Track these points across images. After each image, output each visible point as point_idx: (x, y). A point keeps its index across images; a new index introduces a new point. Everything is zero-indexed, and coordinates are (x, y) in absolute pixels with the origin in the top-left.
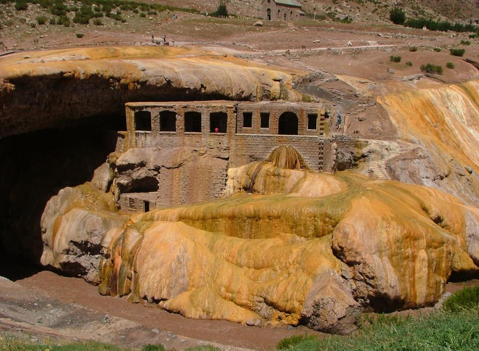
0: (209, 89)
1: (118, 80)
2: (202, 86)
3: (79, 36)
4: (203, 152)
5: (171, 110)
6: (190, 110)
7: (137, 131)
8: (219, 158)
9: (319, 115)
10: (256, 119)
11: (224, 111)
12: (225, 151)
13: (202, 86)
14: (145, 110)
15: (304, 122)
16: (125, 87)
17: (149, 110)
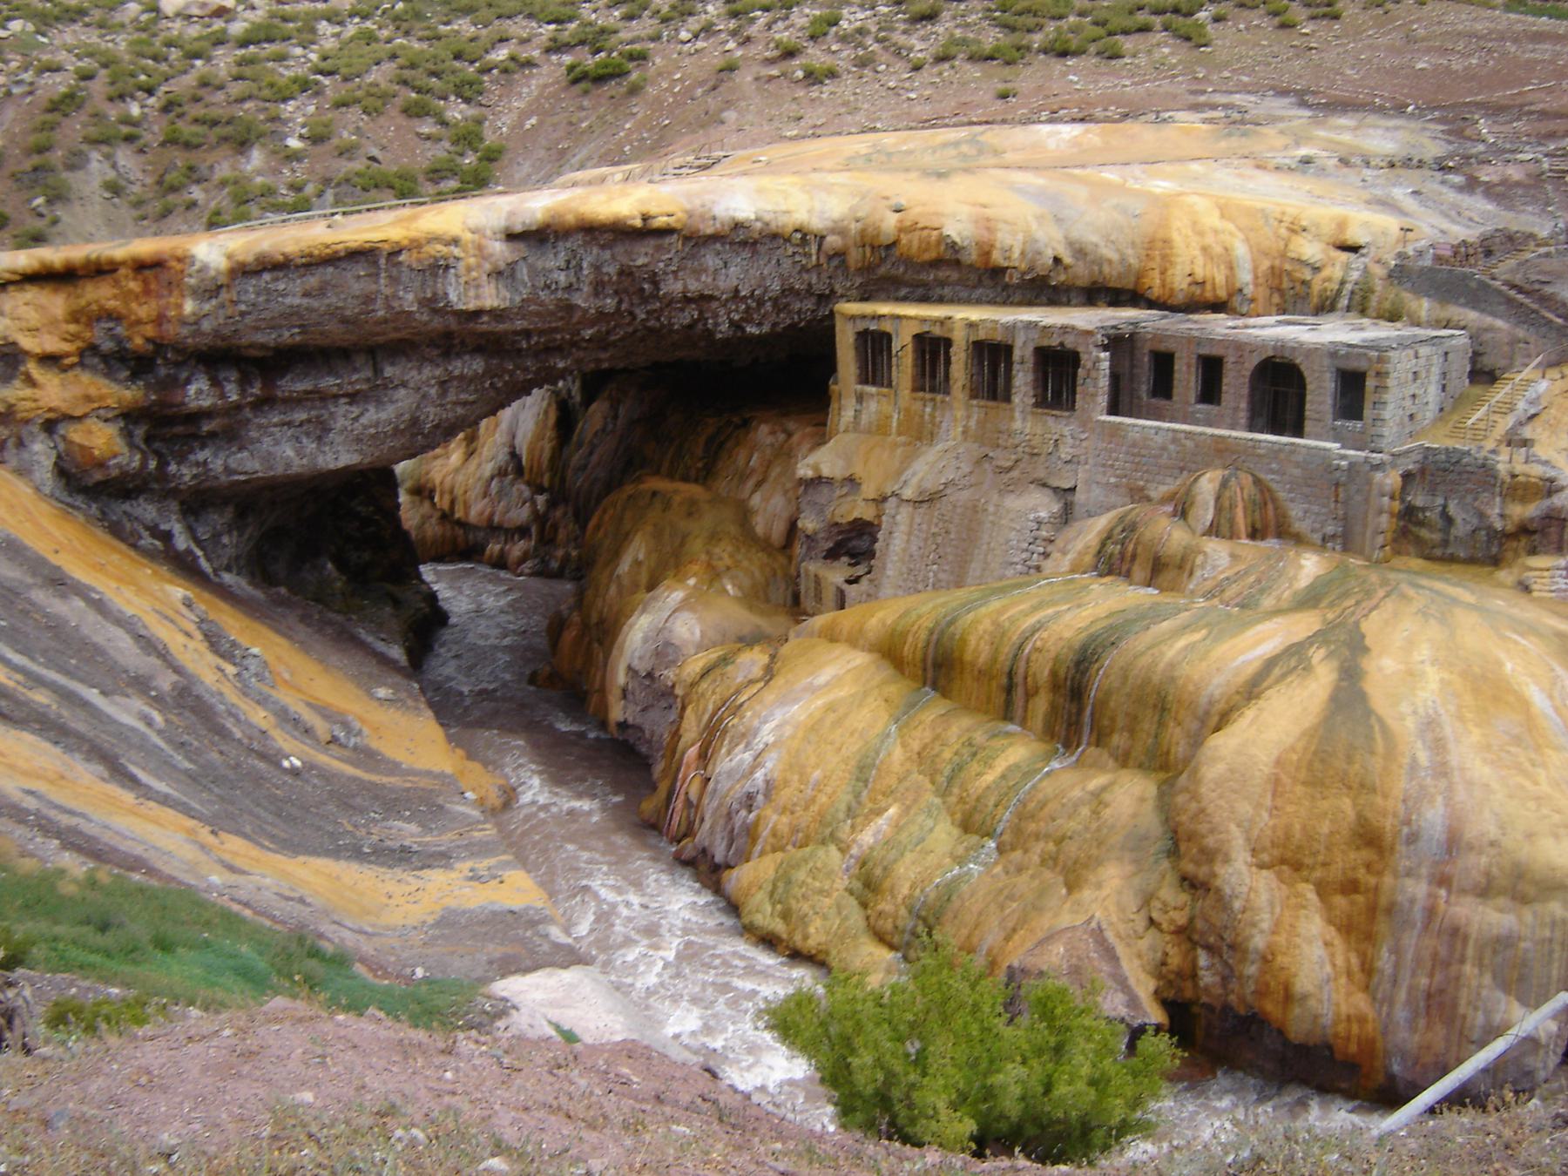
0: (1082, 274)
1: (821, 238)
2: (1057, 260)
3: (1004, 96)
4: (1009, 464)
5: (937, 331)
6: (982, 335)
7: (859, 387)
8: (1044, 485)
9: (1371, 374)
10: (1186, 378)
11: (1070, 342)
12: (1069, 467)
13: (1057, 260)
14: (873, 327)
15: (1321, 394)
16: (840, 255)
17: (887, 326)
